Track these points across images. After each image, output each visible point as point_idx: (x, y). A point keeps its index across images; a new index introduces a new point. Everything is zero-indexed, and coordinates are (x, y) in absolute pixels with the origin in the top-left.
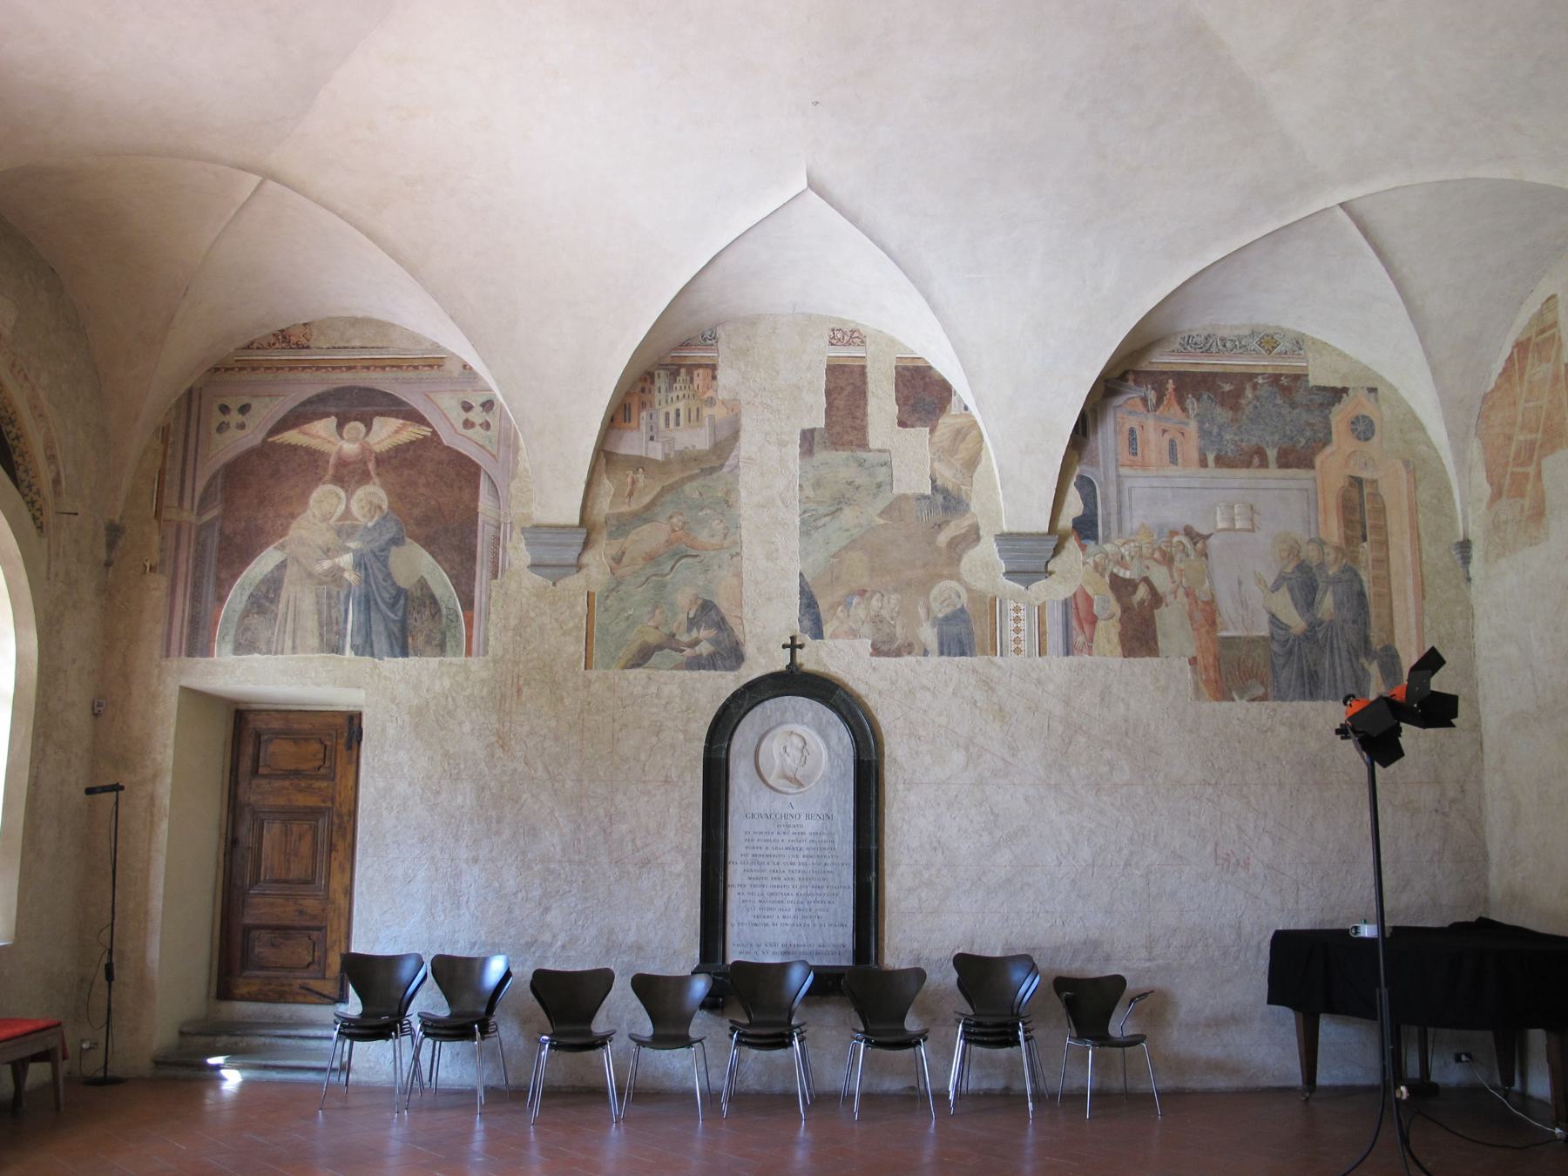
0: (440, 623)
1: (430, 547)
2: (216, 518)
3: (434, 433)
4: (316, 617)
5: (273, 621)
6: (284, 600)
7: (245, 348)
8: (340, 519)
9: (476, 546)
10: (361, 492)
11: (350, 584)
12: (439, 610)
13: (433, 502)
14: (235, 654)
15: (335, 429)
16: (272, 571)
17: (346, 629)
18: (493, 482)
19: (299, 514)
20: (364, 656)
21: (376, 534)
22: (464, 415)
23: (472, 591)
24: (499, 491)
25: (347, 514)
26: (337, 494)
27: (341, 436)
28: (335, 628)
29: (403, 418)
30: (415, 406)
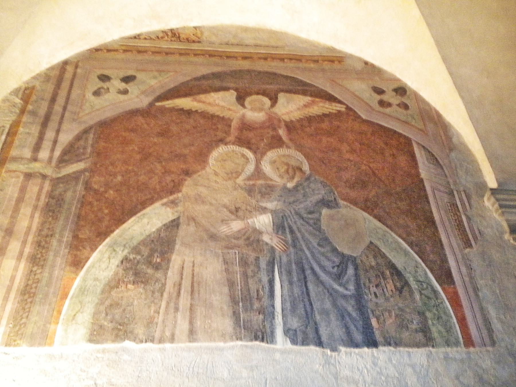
0: (413, 300)
1: (373, 210)
2: (83, 171)
3: (348, 108)
4: (226, 290)
5: (157, 294)
6: (176, 267)
7: (131, 38)
8: (249, 179)
9: (431, 212)
10: (271, 155)
11: (272, 250)
12: (406, 283)
13: (364, 167)
14: (91, 341)
15: (235, 100)
16: (159, 230)
17: (273, 306)
18: (429, 152)
19: (195, 172)
20: (308, 344)
21: (300, 196)
22: (378, 97)
23: (444, 260)
24: (440, 160)
25: (258, 173)
26: (243, 155)
27: (243, 106)
28: (256, 305)
29: (311, 96)
30: (323, 88)
